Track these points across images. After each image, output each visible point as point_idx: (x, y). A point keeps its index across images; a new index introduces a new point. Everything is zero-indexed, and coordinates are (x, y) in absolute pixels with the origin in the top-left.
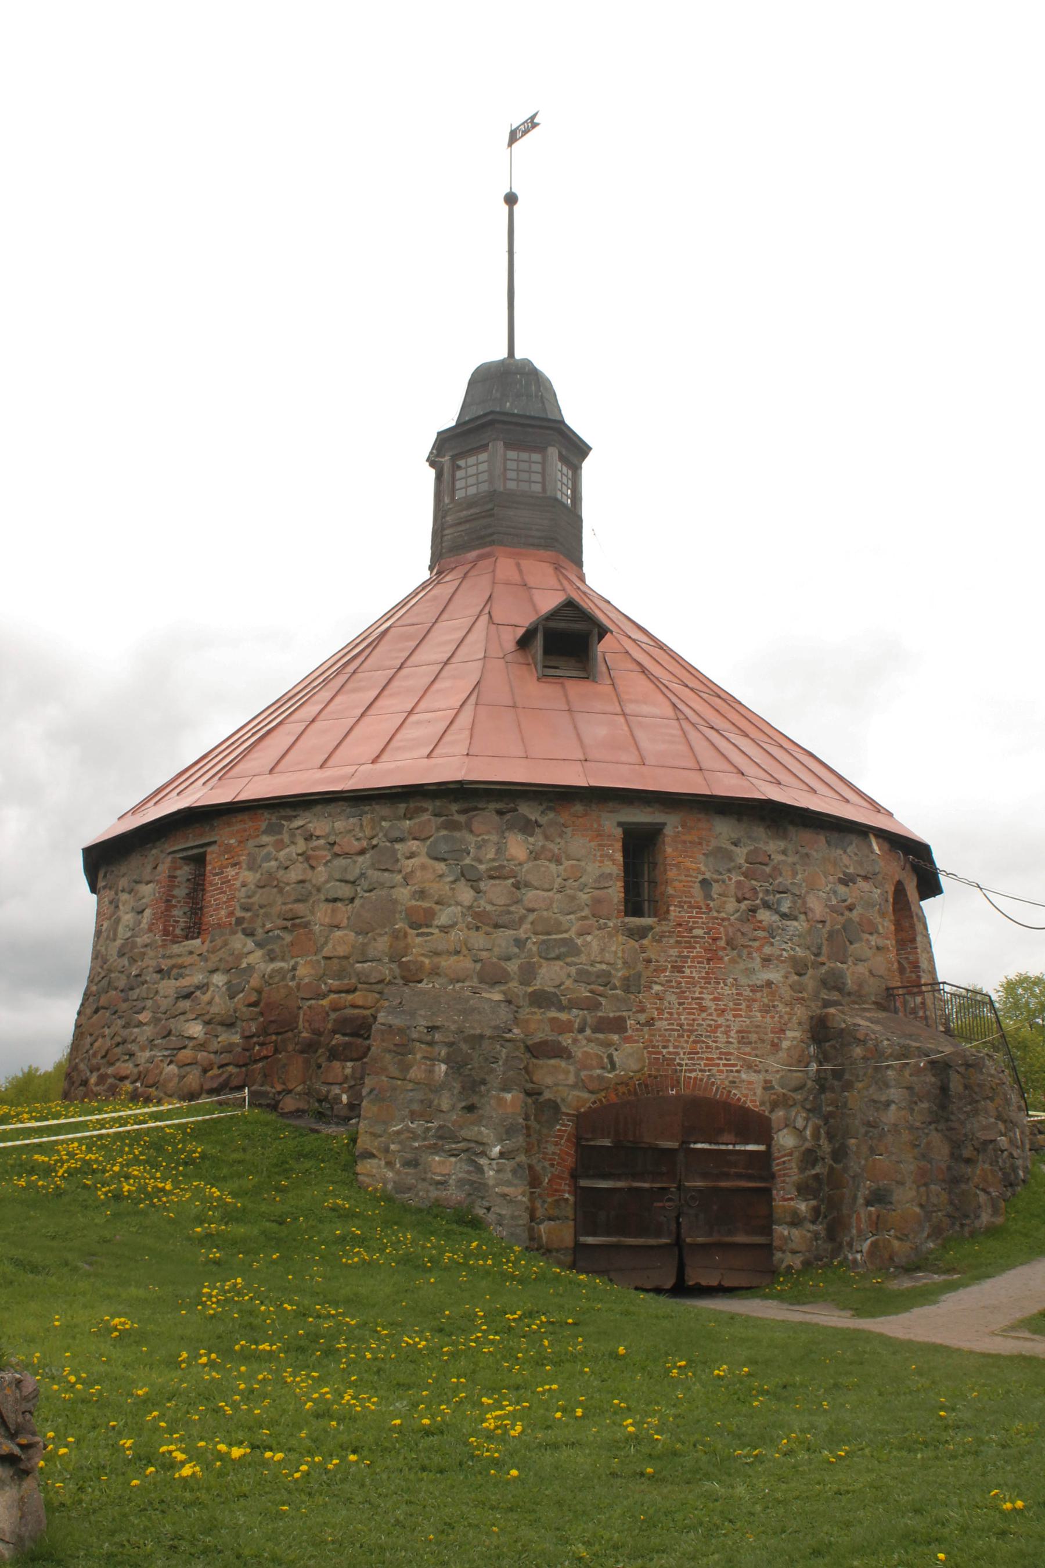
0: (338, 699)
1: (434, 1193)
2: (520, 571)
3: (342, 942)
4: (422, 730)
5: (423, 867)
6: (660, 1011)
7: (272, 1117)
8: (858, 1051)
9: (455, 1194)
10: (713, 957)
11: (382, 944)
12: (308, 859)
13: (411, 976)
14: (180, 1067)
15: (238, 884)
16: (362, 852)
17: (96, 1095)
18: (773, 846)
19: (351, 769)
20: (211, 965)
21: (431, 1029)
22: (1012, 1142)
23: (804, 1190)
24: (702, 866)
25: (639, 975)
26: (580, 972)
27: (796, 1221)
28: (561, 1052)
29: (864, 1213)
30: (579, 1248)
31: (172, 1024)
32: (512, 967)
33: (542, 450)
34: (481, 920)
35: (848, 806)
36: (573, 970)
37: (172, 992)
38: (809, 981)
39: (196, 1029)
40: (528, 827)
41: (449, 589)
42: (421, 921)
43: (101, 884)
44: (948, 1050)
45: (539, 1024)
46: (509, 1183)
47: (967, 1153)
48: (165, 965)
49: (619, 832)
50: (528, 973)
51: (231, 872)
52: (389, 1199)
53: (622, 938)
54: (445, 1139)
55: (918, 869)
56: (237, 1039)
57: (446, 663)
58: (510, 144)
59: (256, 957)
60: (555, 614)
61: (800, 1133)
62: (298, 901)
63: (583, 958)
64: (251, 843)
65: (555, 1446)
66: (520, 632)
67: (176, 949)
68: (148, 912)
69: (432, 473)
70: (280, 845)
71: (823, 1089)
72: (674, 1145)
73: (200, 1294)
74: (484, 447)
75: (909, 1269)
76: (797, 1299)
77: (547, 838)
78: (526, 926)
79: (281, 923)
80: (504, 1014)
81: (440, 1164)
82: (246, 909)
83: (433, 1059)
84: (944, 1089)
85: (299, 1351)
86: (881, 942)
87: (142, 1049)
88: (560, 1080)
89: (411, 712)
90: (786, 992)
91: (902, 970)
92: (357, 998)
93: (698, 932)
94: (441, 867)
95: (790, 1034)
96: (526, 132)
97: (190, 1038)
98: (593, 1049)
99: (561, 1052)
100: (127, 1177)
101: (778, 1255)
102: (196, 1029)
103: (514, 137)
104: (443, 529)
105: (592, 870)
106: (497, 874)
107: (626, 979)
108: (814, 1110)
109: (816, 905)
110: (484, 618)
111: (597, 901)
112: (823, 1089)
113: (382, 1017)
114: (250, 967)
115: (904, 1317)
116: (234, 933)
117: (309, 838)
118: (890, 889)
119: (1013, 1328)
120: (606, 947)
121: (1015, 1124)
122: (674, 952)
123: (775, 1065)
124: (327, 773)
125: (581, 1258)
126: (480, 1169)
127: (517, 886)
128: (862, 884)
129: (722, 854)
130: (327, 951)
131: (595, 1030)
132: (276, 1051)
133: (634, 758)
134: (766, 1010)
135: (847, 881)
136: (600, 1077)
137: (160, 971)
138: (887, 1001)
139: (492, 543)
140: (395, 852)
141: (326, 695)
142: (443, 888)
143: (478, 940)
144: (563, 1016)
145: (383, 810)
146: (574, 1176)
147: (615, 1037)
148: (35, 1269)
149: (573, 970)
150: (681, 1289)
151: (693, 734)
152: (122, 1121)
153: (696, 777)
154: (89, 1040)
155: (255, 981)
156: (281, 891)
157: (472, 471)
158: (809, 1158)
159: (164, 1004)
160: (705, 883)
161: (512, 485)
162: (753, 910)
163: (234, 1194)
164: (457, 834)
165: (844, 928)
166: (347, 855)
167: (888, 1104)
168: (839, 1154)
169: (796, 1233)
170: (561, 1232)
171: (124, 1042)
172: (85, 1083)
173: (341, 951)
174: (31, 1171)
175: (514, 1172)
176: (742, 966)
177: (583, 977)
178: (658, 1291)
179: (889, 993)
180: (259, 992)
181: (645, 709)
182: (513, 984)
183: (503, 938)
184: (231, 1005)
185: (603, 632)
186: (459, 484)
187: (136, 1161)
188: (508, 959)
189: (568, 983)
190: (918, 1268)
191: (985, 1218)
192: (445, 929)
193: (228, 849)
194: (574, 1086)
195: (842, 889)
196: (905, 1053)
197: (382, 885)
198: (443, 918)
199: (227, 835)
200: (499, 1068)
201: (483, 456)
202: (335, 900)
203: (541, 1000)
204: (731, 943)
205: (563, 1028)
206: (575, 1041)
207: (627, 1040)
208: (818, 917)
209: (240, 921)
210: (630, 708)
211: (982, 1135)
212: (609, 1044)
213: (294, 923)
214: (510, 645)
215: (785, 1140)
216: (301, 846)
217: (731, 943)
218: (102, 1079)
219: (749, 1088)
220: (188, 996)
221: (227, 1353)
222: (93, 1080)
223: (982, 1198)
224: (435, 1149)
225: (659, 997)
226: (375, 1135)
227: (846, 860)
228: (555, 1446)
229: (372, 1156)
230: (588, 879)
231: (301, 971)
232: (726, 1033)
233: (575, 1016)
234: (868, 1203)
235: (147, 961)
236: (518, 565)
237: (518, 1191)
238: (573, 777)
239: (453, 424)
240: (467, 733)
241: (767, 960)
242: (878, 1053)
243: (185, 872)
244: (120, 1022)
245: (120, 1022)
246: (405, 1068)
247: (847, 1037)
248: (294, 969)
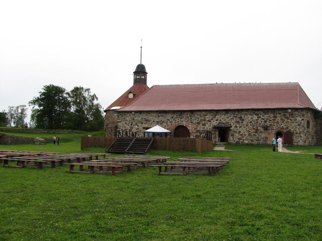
3: (111, 120)
54: (110, 134)
213: (109, 119)
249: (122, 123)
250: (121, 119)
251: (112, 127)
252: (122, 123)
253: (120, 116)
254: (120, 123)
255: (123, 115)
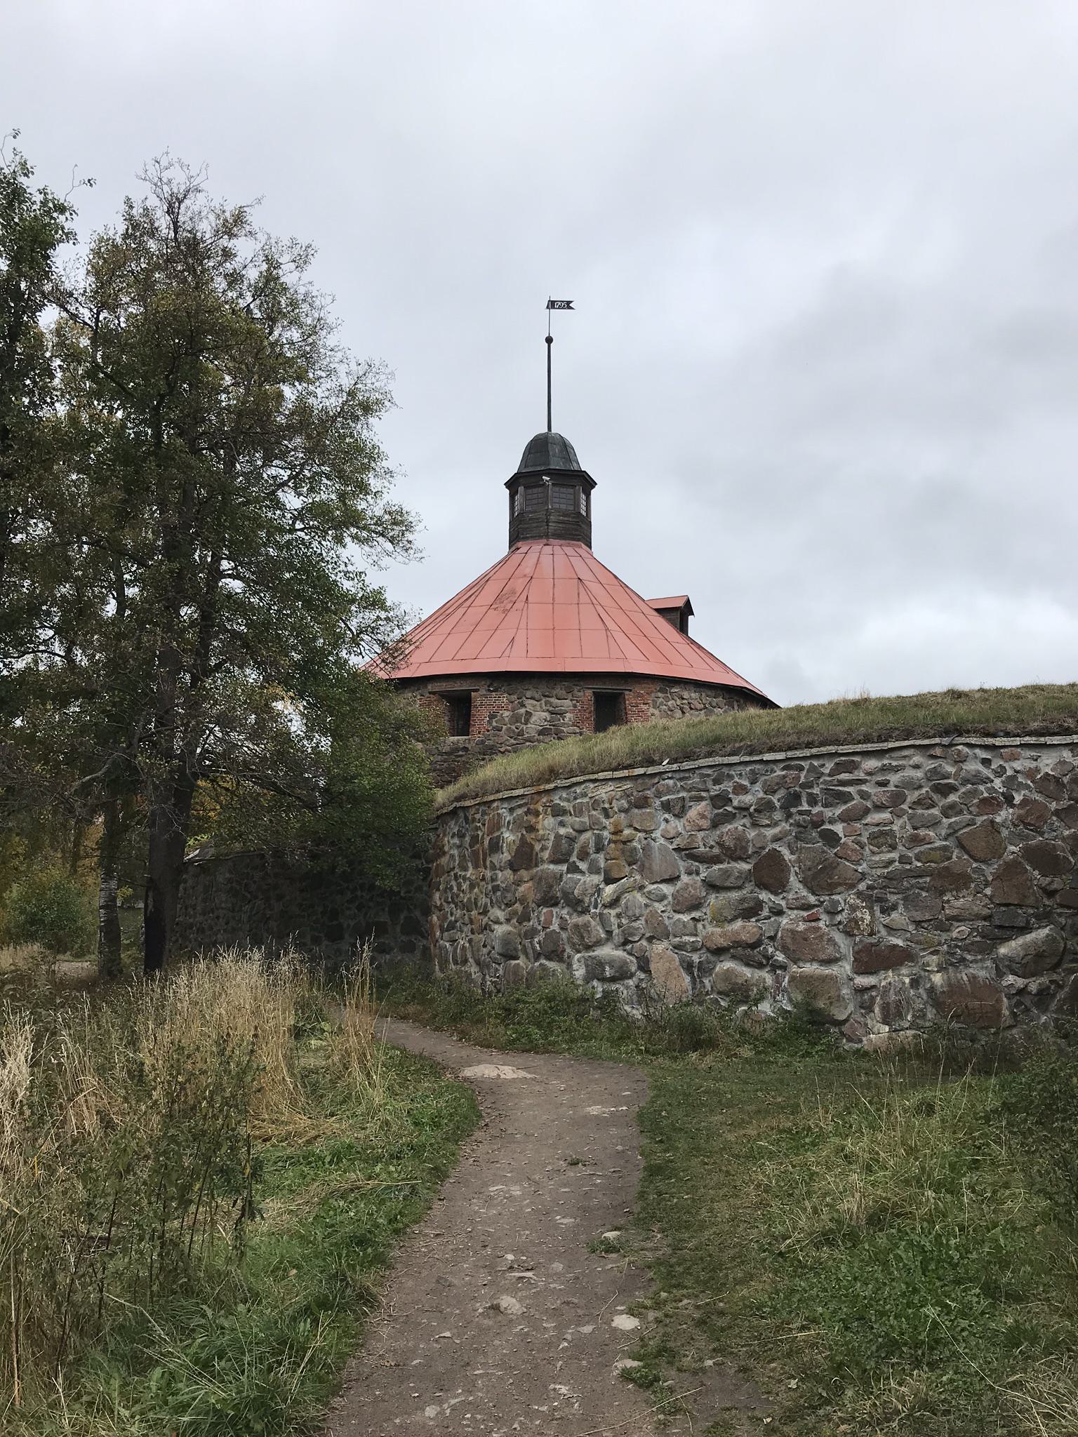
12: (682, 709)
103: (552, 305)
193: (639, 695)
201: (571, 491)
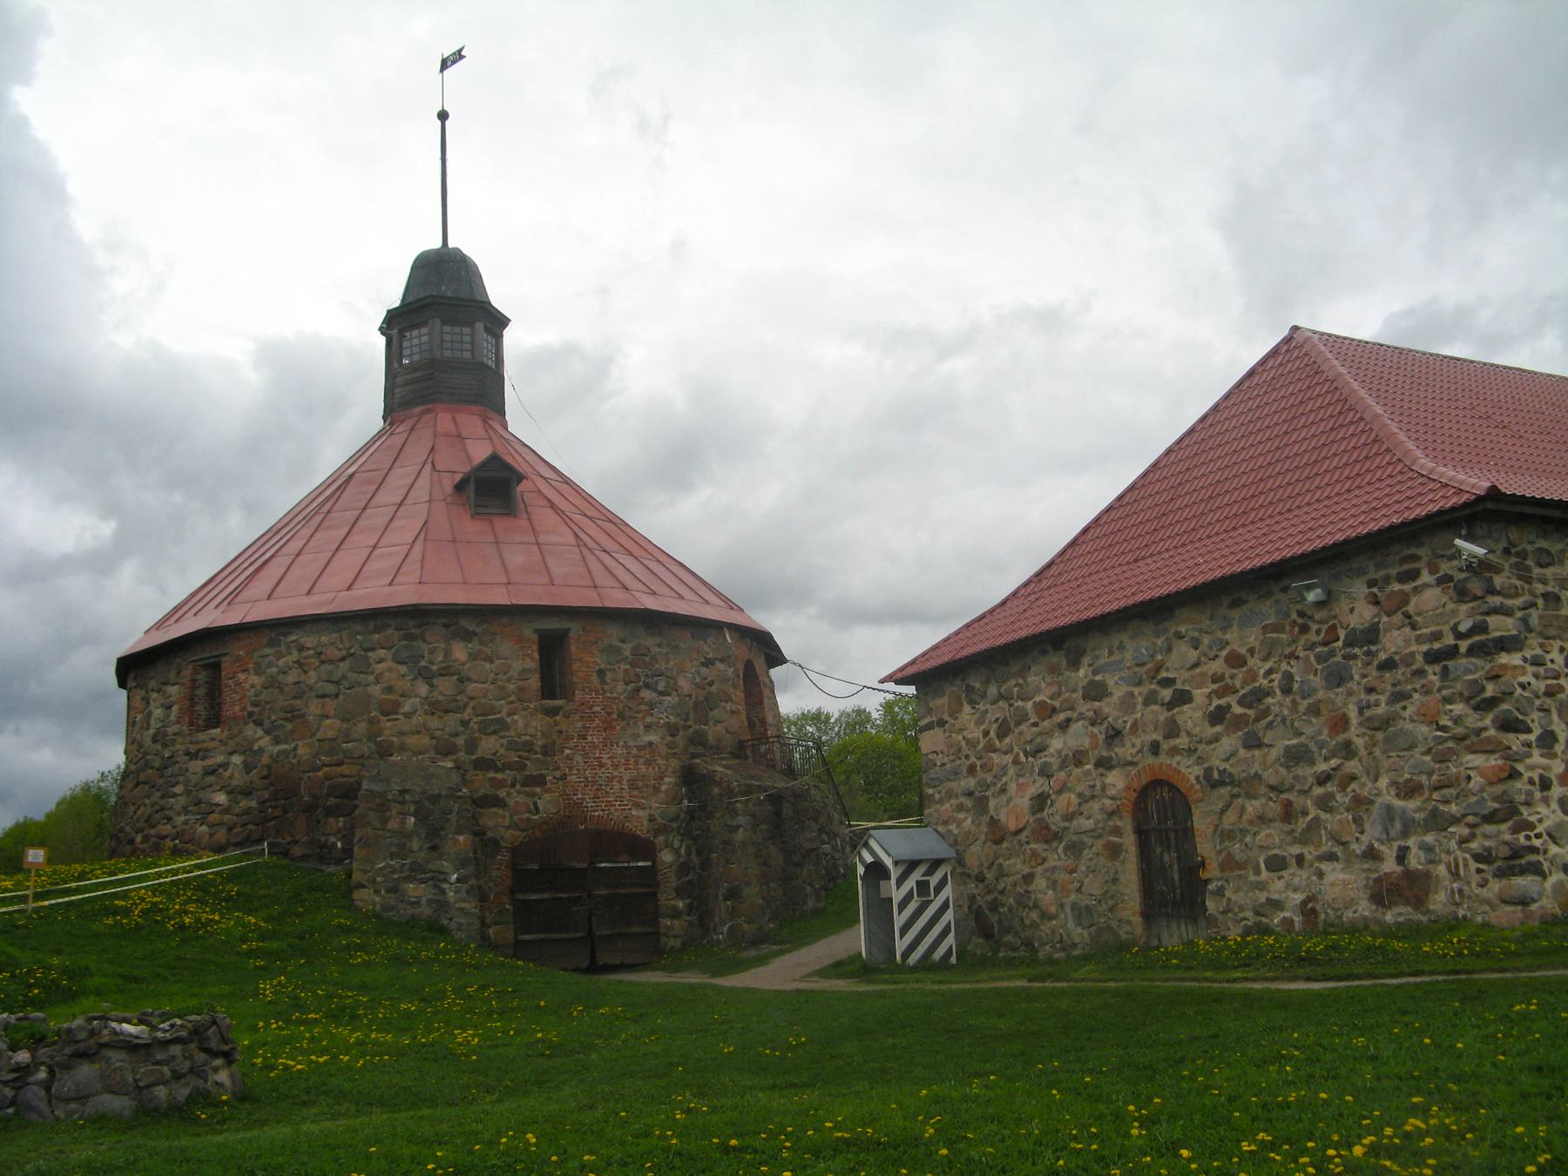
0: (318, 535)
1: (411, 911)
2: (456, 424)
3: (331, 728)
4: (384, 562)
5: (390, 669)
6: (571, 769)
7: (286, 862)
8: (716, 790)
9: (426, 911)
10: (608, 727)
11: (361, 728)
13: (384, 751)
14: (210, 826)
15: (247, 685)
16: (343, 659)
17: (143, 851)
18: (651, 642)
19: (331, 596)
20: (229, 749)
21: (403, 792)
22: (834, 848)
23: (680, 892)
24: (599, 660)
25: (554, 743)
26: (510, 743)
27: (676, 914)
28: (499, 802)
29: (724, 906)
30: (518, 944)
31: (202, 794)
32: (460, 741)
33: (470, 324)
34: (435, 708)
35: (708, 608)
36: (505, 741)
37: (199, 770)
38: (680, 740)
39: (221, 798)
40: (467, 636)
41: (397, 441)
42: (390, 710)
43: (132, 684)
44: (781, 785)
45: (481, 782)
46: (464, 901)
47: (796, 858)
48: (192, 748)
49: (535, 637)
50: (472, 745)
51: (241, 676)
52: (377, 916)
53: (540, 716)
54: (417, 872)
55: (766, 649)
56: (253, 804)
57: (400, 505)
58: (442, 70)
59: (265, 742)
60: (484, 465)
61: (677, 851)
62: (295, 698)
63: (512, 733)
64: (256, 654)
65: (497, 1046)
66: (458, 477)
67: (201, 736)
68: (175, 708)
69: (383, 340)
70: (279, 655)
71: (692, 818)
72: (585, 865)
73: (258, 989)
74: (424, 324)
75: (754, 944)
76: (677, 969)
77: (481, 643)
78: (469, 710)
79: (282, 715)
80: (455, 778)
81: (413, 889)
82: (255, 704)
83: (405, 814)
84: (778, 814)
85: (335, 1016)
86: (734, 707)
87: (179, 814)
88: (497, 822)
89: (375, 547)
90: (664, 750)
91: (751, 725)
92: (344, 769)
93: (597, 709)
94: (403, 669)
95: (667, 780)
96: (454, 62)
97: (217, 805)
98: (521, 799)
99: (499, 802)
100: (186, 913)
101: (664, 939)
102: (221, 798)
103: (445, 65)
104: (394, 378)
105: (517, 666)
106: (446, 672)
107: (544, 746)
108: (686, 834)
109: (684, 683)
110: (428, 467)
111: (521, 689)
112: (692, 818)
113: (365, 785)
114: (261, 750)
115: (743, 976)
116: (246, 723)
117: (301, 649)
118: (741, 667)
119: (809, 975)
120: (529, 724)
121: (836, 835)
122: (579, 725)
123: (656, 804)
124: (314, 598)
125: (520, 949)
126: (443, 892)
127: (461, 681)
128: (720, 666)
129: (612, 650)
130: (319, 736)
131: (524, 784)
132: (285, 812)
133: (545, 580)
134: (648, 763)
135: (708, 663)
136: (529, 819)
137: (188, 754)
138: (739, 751)
139: (433, 401)
140: (367, 658)
141: (307, 532)
142: (404, 685)
143: (434, 722)
144: (499, 776)
145: (359, 628)
146: (512, 892)
147: (538, 790)
148: (137, 980)
149: (505, 741)
150: (594, 968)
151: (591, 560)
152: (175, 872)
153: (592, 594)
154: (132, 808)
155: (265, 760)
156: (282, 690)
157: (416, 341)
158: (684, 868)
159: (194, 779)
160: (601, 673)
161: (447, 353)
162: (637, 690)
163: (266, 921)
164: (415, 643)
165: (706, 698)
166: (331, 662)
167: (738, 827)
168: (705, 864)
169: (676, 923)
170: (501, 932)
171: (163, 809)
172: (132, 842)
173: (331, 734)
174: (115, 913)
175: (468, 892)
176: (630, 732)
177: (512, 746)
178: (576, 970)
179: (741, 745)
180: (269, 767)
181: (554, 539)
182: (461, 754)
183: (452, 720)
184: (247, 778)
185: (520, 478)
186: (406, 352)
187: (189, 901)
188: (457, 735)
189: (502, 751)
190: (763, 942)
191: (810, 904)
192: (408, 715)
193: (239, 659)
194: (509, 827)
195: (704, 670)
196: (748, 791)
197: (359, 684)
198: (407, 708)
199: (238, 649)
200: (453, 817)
201: (424, 330)
202: (324, 696)
203: (483, 764)
204: (621, 716)
205: (499, 784)
206: (509, 794)
207: (549, 791)
208: (686, 692)
209: (251, 714)
210: (543, 538)
211: (807, 845)
212: (534, 795)
213: (293, 714)
214: (449, 490)
215: (667, 857)
216: (295, 656)
217: (621, 716)
218: (146, 839)
219: (638, 820)
220: (213, 772)
221: (288, 1022)
222: (138, 839)
223: (809, 889)
224: (409, 879)
225: (569, 758)
226: (365, 872)
227: (706, 648)
228: (497, 1046)
229: (363, 886)
230: (514, 673)
231: (300, 751)
232: (620, 782)
233: (507, 775)
234: (726, 899)
235: (177, 747)
236: (454, 419)
237: (471, 906)
238: (499, 597)
239: (397, 304)
240: (418, 565)
241: (648, 727)
242: (730, 792)
243: (203, 676)
244: (158, 794)
245: (158, 794)
246: (385, 821)
247: (709, 779)
248: (295, 749)
249: (1537, 662)
250: (1518, 602)
251: (435, 799)
252: (1537, 662)
253: (1497, 570)
254: (1515, 659)
255: (1523, 555)
